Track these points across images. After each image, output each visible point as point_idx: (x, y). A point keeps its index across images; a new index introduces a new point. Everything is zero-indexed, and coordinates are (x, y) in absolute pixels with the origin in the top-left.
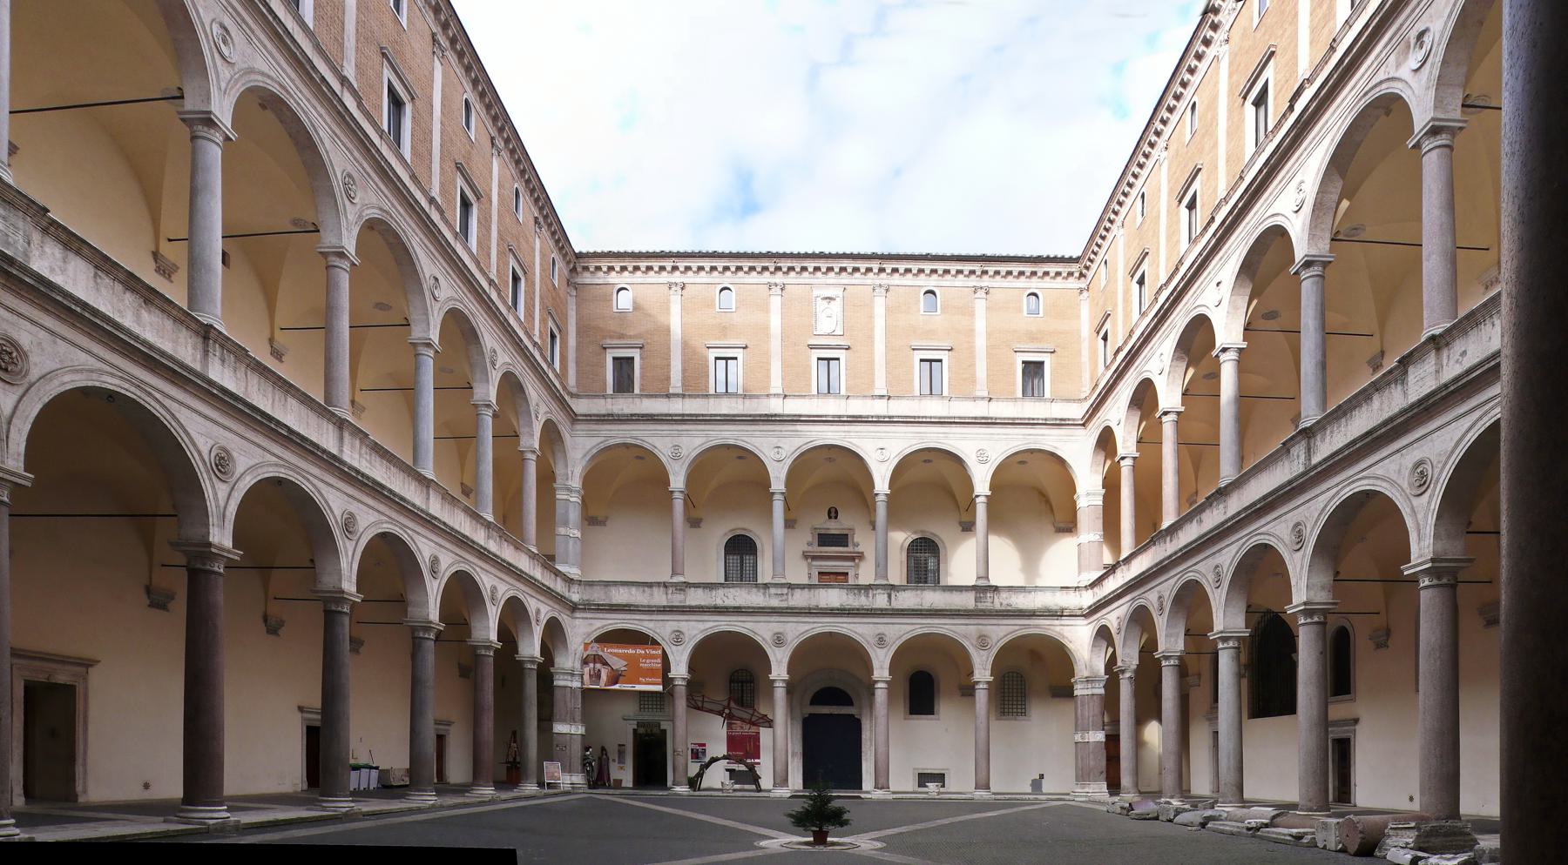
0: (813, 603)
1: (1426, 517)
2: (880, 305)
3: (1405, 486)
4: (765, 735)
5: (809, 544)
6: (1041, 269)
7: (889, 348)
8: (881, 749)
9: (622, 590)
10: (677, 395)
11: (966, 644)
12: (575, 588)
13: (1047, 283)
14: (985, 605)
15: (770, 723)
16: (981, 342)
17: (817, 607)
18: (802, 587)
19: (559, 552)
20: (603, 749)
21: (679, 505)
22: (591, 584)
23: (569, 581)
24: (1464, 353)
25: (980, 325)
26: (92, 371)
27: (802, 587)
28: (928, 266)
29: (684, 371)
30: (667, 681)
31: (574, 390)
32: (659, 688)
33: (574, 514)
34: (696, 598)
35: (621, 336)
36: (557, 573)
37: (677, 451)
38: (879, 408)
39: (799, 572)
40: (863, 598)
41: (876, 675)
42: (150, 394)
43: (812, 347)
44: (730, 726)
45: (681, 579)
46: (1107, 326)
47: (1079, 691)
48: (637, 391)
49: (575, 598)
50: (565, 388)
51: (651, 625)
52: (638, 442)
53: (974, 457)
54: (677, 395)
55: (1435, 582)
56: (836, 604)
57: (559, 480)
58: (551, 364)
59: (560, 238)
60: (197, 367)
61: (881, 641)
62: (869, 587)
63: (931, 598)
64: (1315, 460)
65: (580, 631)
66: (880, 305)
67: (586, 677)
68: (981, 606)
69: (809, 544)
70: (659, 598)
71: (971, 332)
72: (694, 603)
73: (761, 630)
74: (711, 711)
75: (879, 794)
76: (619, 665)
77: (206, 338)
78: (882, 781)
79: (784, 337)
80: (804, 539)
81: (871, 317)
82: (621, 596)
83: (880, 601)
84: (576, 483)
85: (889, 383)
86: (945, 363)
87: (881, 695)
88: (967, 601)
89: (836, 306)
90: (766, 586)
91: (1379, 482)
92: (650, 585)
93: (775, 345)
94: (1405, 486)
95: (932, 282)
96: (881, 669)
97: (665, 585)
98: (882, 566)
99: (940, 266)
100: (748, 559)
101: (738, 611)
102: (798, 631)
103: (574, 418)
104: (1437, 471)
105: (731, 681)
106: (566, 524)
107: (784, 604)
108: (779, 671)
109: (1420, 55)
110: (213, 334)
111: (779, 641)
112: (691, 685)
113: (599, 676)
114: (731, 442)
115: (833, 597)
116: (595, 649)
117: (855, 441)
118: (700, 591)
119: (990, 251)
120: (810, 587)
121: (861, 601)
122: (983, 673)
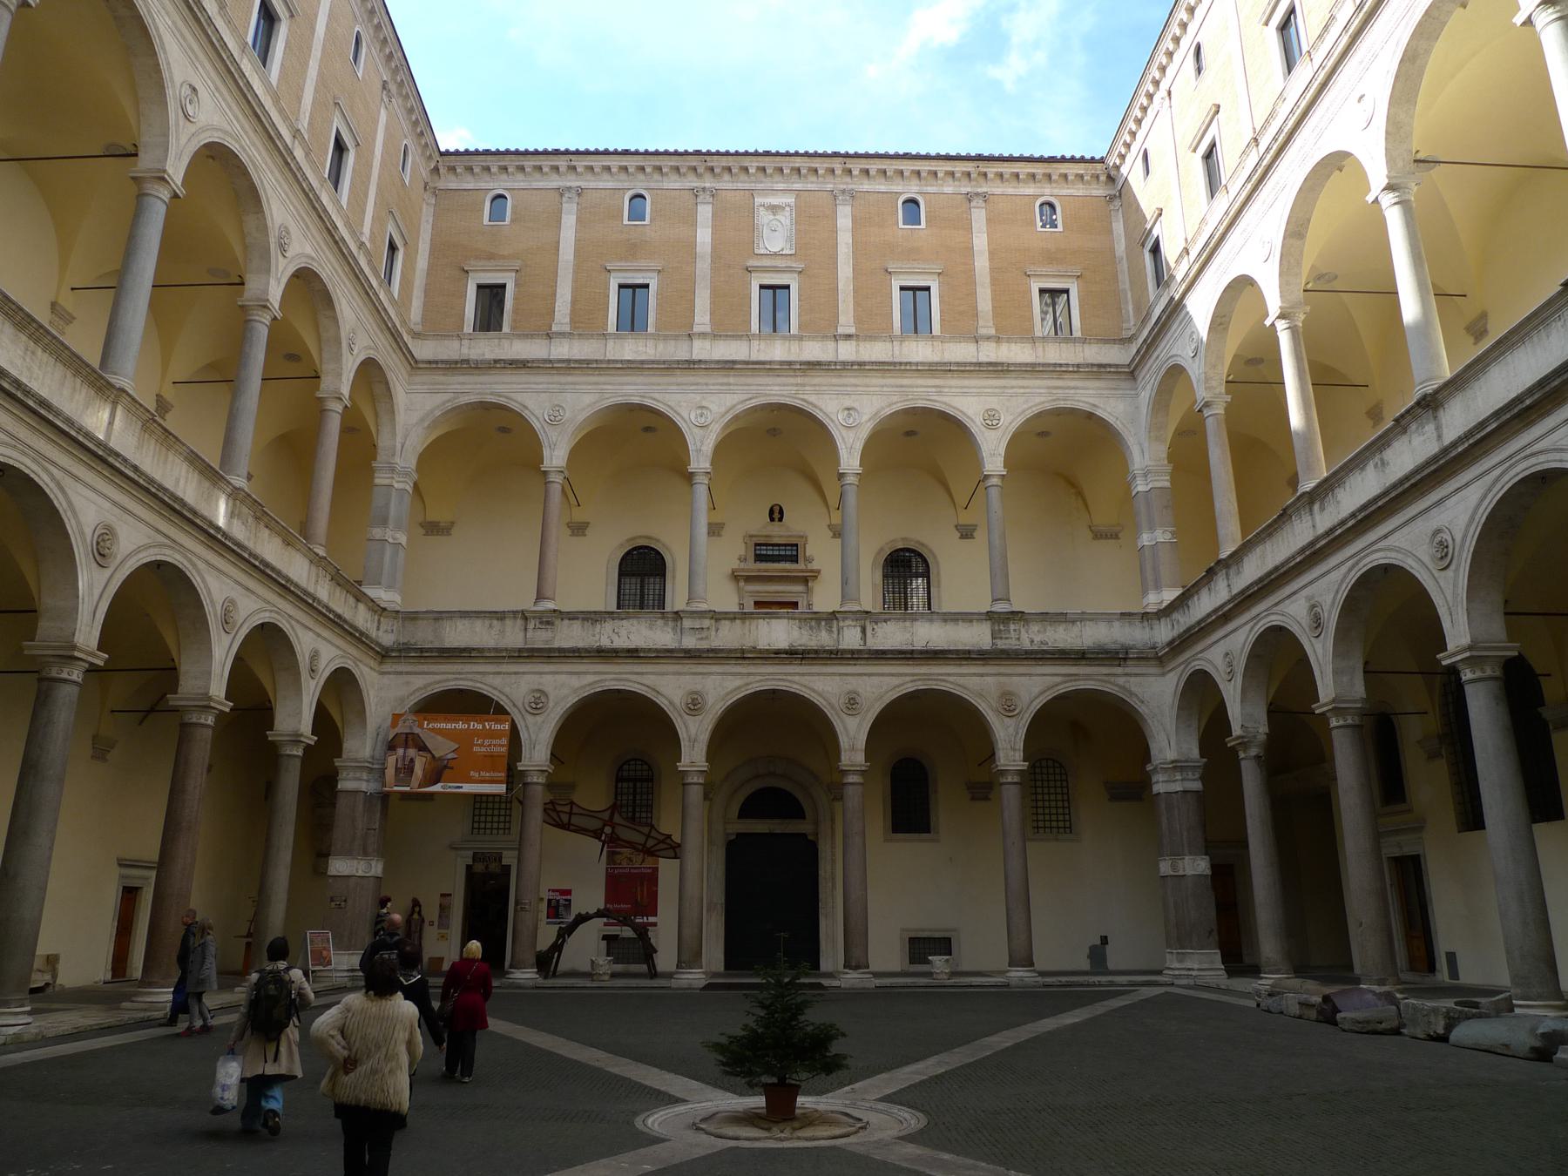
0: (748, 643)
2: (844, 218)
4: (667, 869)
10: (562, 335)
11: (982, 706)
12: (386, 623)
16: (982, 263)
17: (754, 649)
20: (416, 903)
23: (379, 610)
25: (980, 241)
29: (574, 302)
30: (513, 776)
31: (418, 328)
32: (501, 789)
33: (399, 508)
34: (571, 636)
35: (491, 257)
37: (559, 413)
39: (725, 598)
40: (824, 634)
44: (612, 856)
45: (550, 605)
47: (1161, 785)
48: (506, 328)
50: (404, 322)
51: (497, 681)
52: (502, 401)
53: (979, 420)
54: (562, 335)
57: (382, 456)
59: (421, 123)
61: (852, 703)
62: (833, 616)
63: (929, 634)
65: (386, 694)
66: (844, 218)
67: (390, 772)
68: (1001, 645)
70: (513, 636)
71: (969, 250)
73: (667, 687)
74: (581, 830)
76: (443, 748)
79: (716, 254)
81: (835, 231)
82: (458, 635)
83: (851, 638)
85: (858, 320)
86: (934, 292)
87: (853, 796)
88: (978, 636)
89: (785, 218)
90: (678, 616)
92: (500, 616)
93: (703, 266)
96: (852, 734)
97: (524, 616)
100: (652, 584)
101: (633, 654)
102: (723, 688)
105: (619, 779)
106: (384, 522)
107: (704, 645)
108: (694, 755)
114: (636, 400)
115: (778, 633)
117: (812, 398)
118: (577, 624)
120: (743, 616)
121: (822, 639)
122: (1010, 751)
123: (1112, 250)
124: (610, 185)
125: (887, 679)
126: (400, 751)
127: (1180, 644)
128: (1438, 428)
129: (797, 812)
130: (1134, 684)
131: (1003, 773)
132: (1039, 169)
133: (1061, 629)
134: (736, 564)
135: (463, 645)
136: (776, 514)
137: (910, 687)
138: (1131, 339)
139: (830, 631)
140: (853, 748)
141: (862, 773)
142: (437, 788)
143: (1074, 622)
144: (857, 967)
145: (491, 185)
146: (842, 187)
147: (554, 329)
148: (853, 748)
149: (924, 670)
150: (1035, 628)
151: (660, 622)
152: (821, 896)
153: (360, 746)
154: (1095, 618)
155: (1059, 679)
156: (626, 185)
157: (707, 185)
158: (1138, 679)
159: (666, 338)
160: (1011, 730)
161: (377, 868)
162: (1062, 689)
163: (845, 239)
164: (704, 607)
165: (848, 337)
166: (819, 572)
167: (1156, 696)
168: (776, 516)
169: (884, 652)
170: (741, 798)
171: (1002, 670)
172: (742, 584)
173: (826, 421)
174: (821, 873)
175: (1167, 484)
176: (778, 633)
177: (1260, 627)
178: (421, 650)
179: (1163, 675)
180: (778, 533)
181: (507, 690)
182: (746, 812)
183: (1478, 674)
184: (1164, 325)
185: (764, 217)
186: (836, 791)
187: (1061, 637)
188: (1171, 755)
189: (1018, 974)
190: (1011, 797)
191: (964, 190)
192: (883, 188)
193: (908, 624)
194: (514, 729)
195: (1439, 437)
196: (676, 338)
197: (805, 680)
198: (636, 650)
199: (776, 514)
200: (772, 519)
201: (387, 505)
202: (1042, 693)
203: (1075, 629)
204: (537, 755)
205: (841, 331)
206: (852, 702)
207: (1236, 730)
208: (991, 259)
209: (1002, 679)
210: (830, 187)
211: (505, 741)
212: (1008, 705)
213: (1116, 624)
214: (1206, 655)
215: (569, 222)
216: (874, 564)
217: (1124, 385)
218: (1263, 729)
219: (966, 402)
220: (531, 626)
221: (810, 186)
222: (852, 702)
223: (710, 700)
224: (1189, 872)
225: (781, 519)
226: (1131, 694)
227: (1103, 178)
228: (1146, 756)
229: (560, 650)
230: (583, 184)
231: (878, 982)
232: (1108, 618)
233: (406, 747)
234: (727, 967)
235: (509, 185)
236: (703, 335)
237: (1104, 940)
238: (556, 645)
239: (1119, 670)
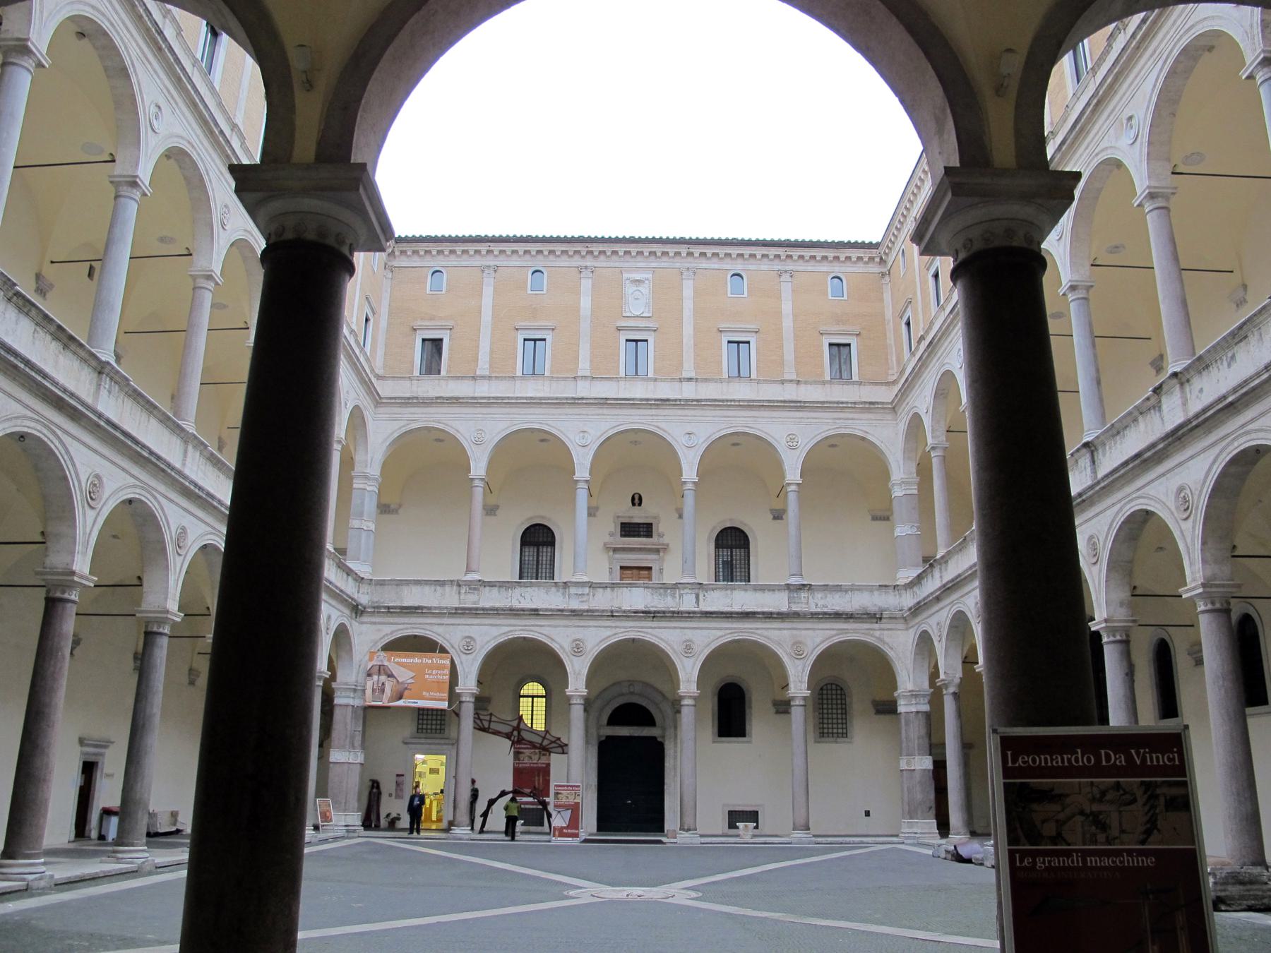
0: (615, 606)
1: (1193, 540)
3: (1173, 509)
5: (611, 535)
6: (843, 254)
7: (696, 329)
9: (416, 589)
10: (483, 377)
11: (780, 652)
12: (364, 588)
13: (849, 268)
15: (563, 748)
16: (788, 323)
18: (604, 586)
19: (351, 547)
21: (478, 493)
22: (382, 583)
23: (360, 580)
24: (1201, 391)
25: (787, 307)
26: (17, 418)
27: (604, 586)
28: (734, 251)
30: (453, 696)
31: (380, 372)
32: (444, 705)
33: (370, 505)
34: (491, 599)
36: (349, 572)
37: (479, 436)
38: (688, 391)
40: (669, 598)
41: (683, 689)
42: (54, 433)
43: (619, 329)
45: (476, 576)
46: (909, 313)
47: (901, 709)
48: (443, 373)
49: (364, 599)
50: (372, 370)
51: (440, 630)
52: (441, 426)
55: (1210, 607)
56: (641, 607)
58: (362, 350)
60: (89, 400)
61: (688, 648)
62: (675, 586)
64: (1100, 475)
67: (369, 692)
68: (795, 608)
69: (611, 535)
70: (450, 599)
71: (778, 314)
72: (488, 605)
75: (684, 838)
76: (404, 675)
77: (100, 373)
78: (688, 821)
80: (608, 528)
82: (412, 597)
83: (687, 603)
84: (375, 470)
87: (687, 715)
88: (779, 602)
89: (645, 289)
90: (566, 585)
91: (1261, 435)
92: (442, 583)
93: (585, 326)
94: (1173, 509)
95: (738, 266)
98: (689, 564)
99: (747, 251)
101: (535, 613)
102: (597, 637)
103: (378, 401)
104: (1196, 497)
106: (360, 515)
107: (586, 607)
109: (1132, 134)
110: (106, 370)
111: (578, 650)
112: (481, 702)
113: (383, 691)
115: (636, 598)
116: (383, 658)
117: (663, 425)
118: (495, 590)
119: (793, 236)
120: (613, 586)
122: (799, 686)
123: (883, 315)
124: (518, 264)
125: (714, 632)
126: (375, 677)
127: (917, 609)
130: (887, 636)
131: (793, 698)
132: (831, 253)
133: (837, 596)
134: (607, 539)
135: (416, 604)
136: (637, 500)
138: (895, 382)
139: (674, 597)
140: (688, 681)
141: (695, 698)
142: (401, 703)
143: (846, 591)
144: (688, 830)
145: (432, 264)
146: (687, 265)
147: (478, 373)
148: (688, 681)
150: (819, 595)
151: (554, 589)
152: (666, 781)
153: (347, 676)
154: (860, 589)
156: (529, 264)
157: (588, 264)
159: (558, 379)
160: (800, 668)
162: (836, 639)
163: (688, 305)
164: (585, 579)
165: (690, 379)
168: (637, 501)
169: (711, 613)
171: (794, 625)
173: (673, 443)
175: (915, 492)
176: (636, 598)
178: (389, 608)
179: (907, 629)
180: (638, 516)
181: (447, 636)
182: (614, 720)
184: (918, 373)
185: (630, 289)
187: (836, 603)
188: (910, 686)
189: (799, 835)
190: (797, 714)
191: (776, 268)
192: (716, 266)
194: (452, 662)
196: (565, 379)
198: (536, 610)
199: (637, 500)
200: (634, 504)
201: (362, 503)
202: (823, 642)
204: (468, 685)
205: (685, 375)
206: (688, 654)
208: (795, 321)
210: (678, 265)
211: (447, 672)
213: (876, 593)
215: (488, 292)
216: (709, 539)
217: (889, 417)
219: (774, 429)
220: (463, 591)
221: (663, 265)
222: (688, 654)
224: (918, 768)
225: (640, 504)
226: (884, 643)
227: (877, 260)
228: (894, 687)
229: (483, 609)
230: (498, 263)
231: (703, 840)
232: (870, 589)
233: (379, 674)
234: (599, 829)
235: (444, 264)
236: (584, 378)
238: (480, 605)
239: (876, 626)
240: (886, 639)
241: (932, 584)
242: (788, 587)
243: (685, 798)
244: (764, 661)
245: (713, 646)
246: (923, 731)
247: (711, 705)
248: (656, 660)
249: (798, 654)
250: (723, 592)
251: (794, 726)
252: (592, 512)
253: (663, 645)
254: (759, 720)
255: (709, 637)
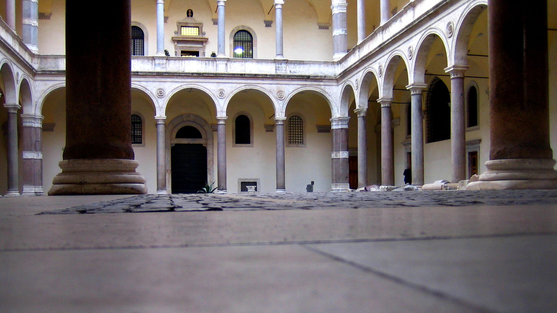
8: (222, 164)
12: (36, 60)
14: (281, 72)
22: (45, 57)
23: (32, 55)
33: (34, 11)
47: (334, 127)
68: (279, 73)
78: (222, 185)
83: (221, 68)
87: (221, 129)
88: (270, 69)
90: (153, 58)
106: (29, 16)
108: (161, 114)
111: (161, 94)
121: (210, 68)
122: (280, 114)
125: (235, 85)
128: (414, 13)
129: (199, 136)
131: (277, 121)
133: (302, 66)
134: (174, 35)
137: (244, 88)
141: (225, 120)
144: (222, 190)
148: (222, 111)
149: (249, 81)
150: (292, 66)
154: (314, 63)
155: (299, 86)
158: (329, 87)
160: (281, 105)
161: (40, 156)
162: (300, 90)
166: (208, 39)
167: (334, 93)
168: (190, 14)
170: (176, 131)
172: (176, 43)
174: (208, 158)
175: (345, 11)
177: (366, 72)
179: (338, 86)
182: (179, 135)
183: (415, 93)
186: (214, 127)
190: (280, 131)
193: (243, 63)
195: (414, 17)
197: (203, 85)
200: (188, 16)
201: (30, 9)
202: (293, 91)
203: (307, 67)
206: (222, 95)
207: (357, 107)
209: (279, 86)
212: (280, 95)
214: (351, 79)
216: (230, 36)
218: (366, 107)
222: (222, 95)
223: (167, 93)
225: (192, 16)
237: (313, 183)
240: (327, 91)
241: (353, 60)
242: (275, 61)
243: (221, 173)
244: (262, 102)
245: (234, 93)
246: (344, 138)
247: (232, 126)
248: (203, 100)
249: (281, 98)
250: (241, 63)
251: (278, 136)
252: (166, 19)
253: (208, 92)
254: (257, 135)
255: (232, 88)
